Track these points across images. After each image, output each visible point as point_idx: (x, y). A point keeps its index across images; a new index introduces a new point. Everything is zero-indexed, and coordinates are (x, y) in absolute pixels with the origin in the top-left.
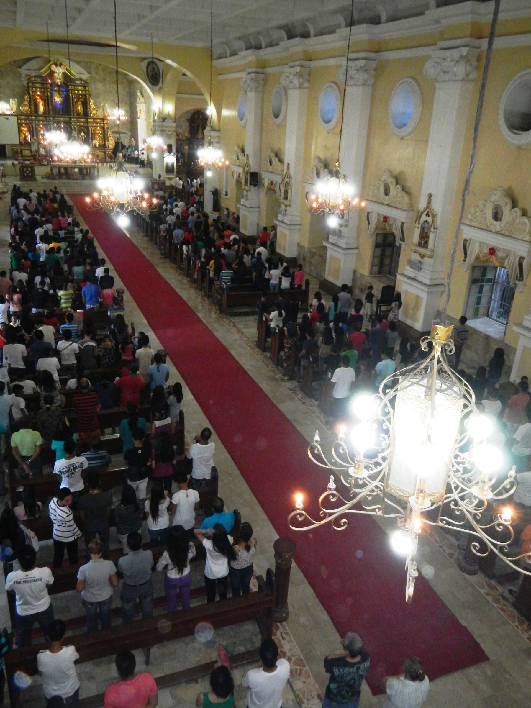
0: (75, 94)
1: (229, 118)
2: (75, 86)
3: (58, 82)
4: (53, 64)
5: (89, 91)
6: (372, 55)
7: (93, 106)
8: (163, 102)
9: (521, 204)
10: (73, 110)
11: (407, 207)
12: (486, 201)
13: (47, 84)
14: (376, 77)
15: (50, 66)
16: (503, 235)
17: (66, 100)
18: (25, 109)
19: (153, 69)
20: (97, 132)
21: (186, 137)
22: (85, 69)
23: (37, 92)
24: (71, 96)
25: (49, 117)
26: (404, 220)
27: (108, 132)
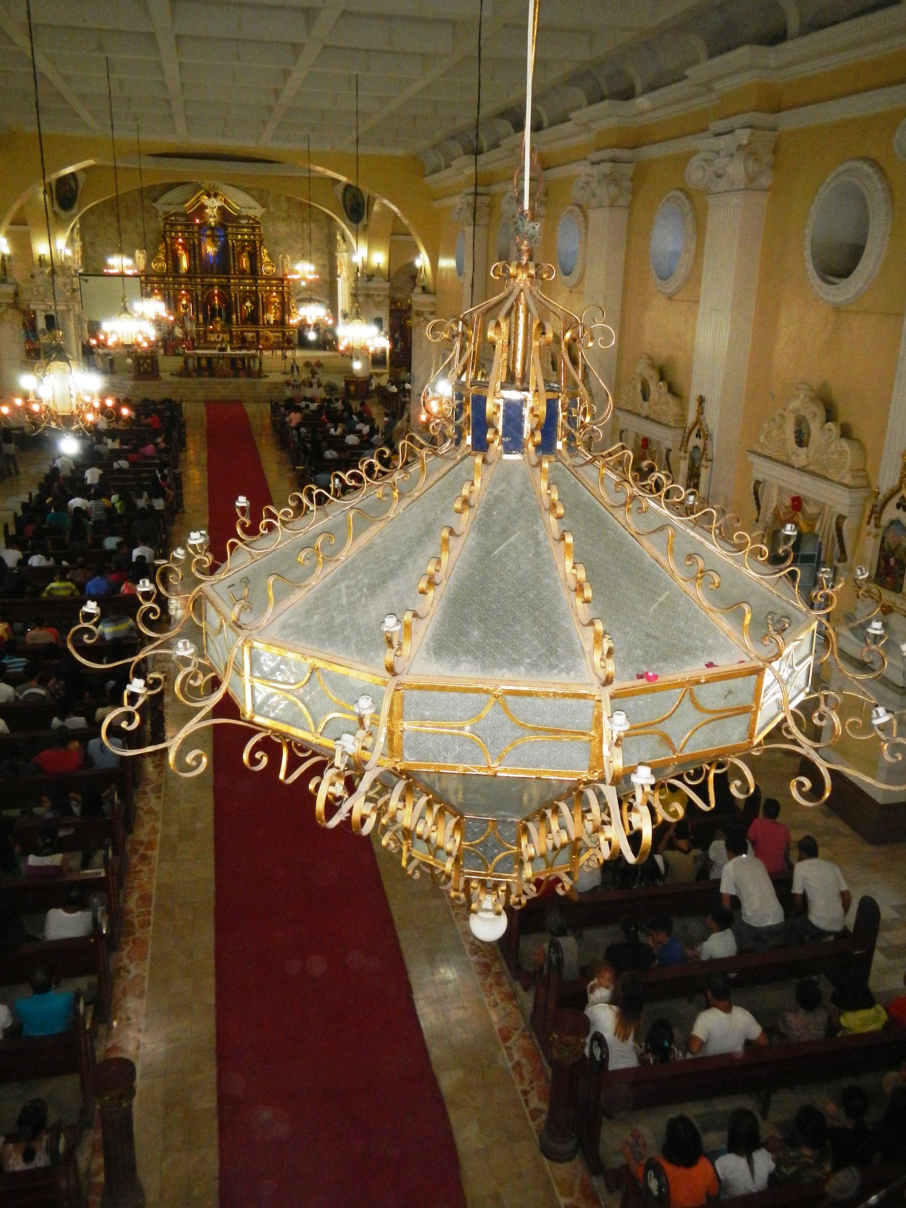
0: (237, 241)
1: (447, 270)
4: (203, 194)
6: (625, 154)
7: (266, 259)
8: (370, 249)
9: (842, 417)
10: (234, 266)
11: (675, 420)
12: (785, 409)
13: (192, 225)
14: (634, 192)
16: (813, 473)
17: (224, 252)
18: (159, 266)
22: (257, 201)
23: (177, 239)
25: (196, 278)
26: (668, 444)
27: (289, 300)
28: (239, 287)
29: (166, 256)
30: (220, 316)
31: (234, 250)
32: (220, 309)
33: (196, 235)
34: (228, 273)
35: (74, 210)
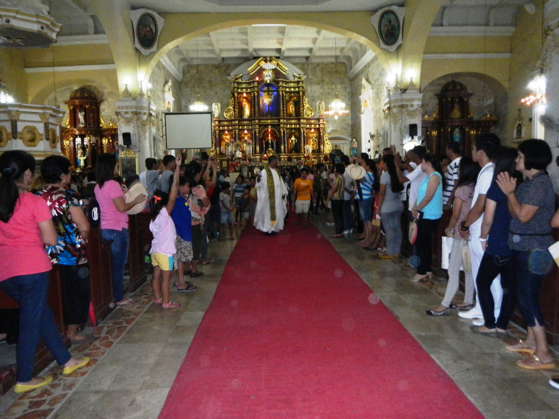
0: (286, 92)
3: (268, 79)
4: (262, 60)
5: (303, 87)
7: (307, 106)
8: (404, 65)
13: (253, 82)
15: (260, 61)
17: (276, 104)
19: (390, 21)
20: (311, 135)
21: (435, 118)
23: (242, 93)
24: (281, 94)
25: (255, 120)
27: (324, 134)
28: (286, 125)
29: (234, 108)
30: (272, 147)
31: (283, 99)
32: (272, 143)
33: (256, 88)
34: (280, 116)
35: (154, 49)
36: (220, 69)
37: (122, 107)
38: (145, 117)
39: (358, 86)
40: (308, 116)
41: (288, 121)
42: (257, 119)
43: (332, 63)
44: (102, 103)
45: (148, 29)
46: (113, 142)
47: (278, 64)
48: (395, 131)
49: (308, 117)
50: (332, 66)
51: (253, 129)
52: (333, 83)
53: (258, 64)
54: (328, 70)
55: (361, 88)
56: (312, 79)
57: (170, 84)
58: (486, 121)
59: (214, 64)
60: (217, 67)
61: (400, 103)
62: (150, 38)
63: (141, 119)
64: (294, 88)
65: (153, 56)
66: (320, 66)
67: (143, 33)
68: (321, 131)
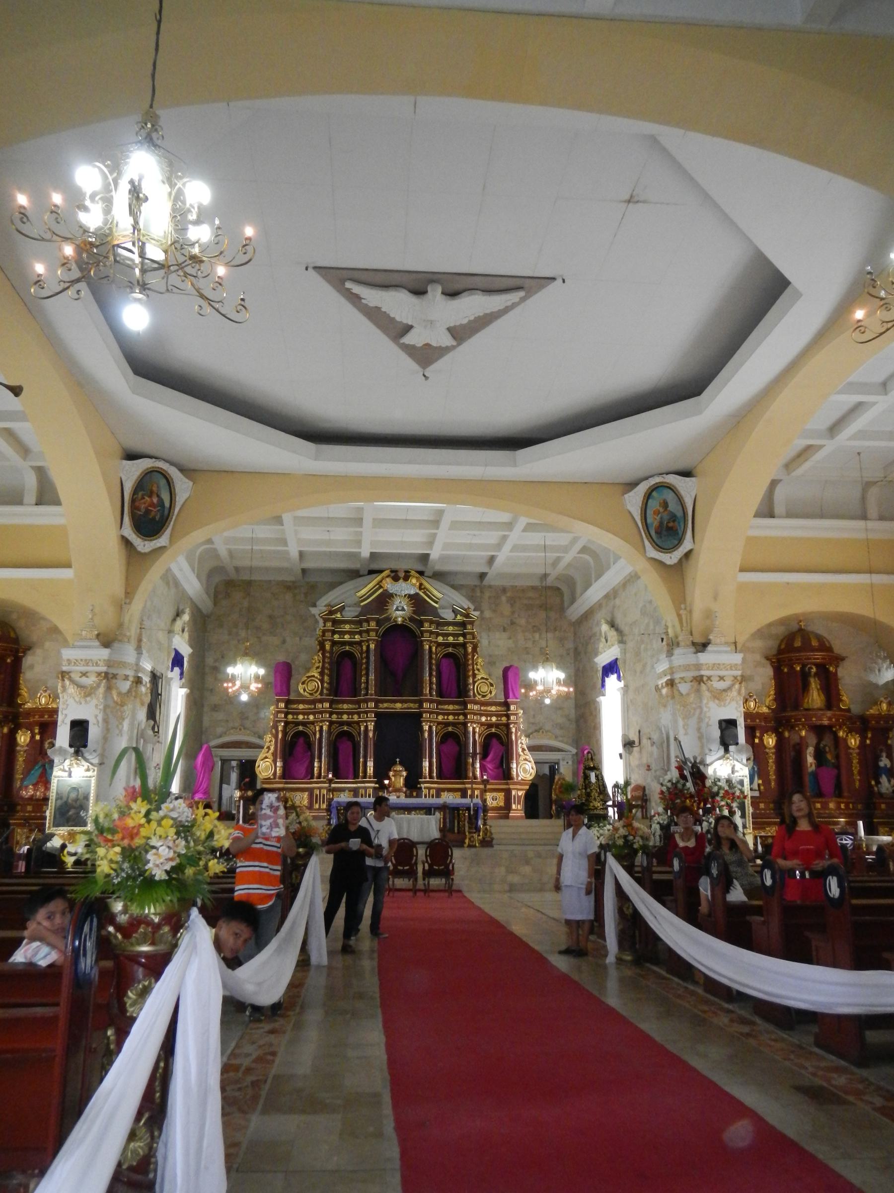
0: (439, 645)
2: (439, 624)
4: (388, 576)
5: (472, 634)
19: (665, 505)
25: (366, 701)
29: (322, 674)
31: (431, 658)
33: (373, 634)
35: (162, 540)
36: (296, 591)
37: (76, 662)
38: (125, 686)
39: (590, 638)
40: (484, 696)
41: (439, 707)
42: (371, 700)
43: (534, 588)
44: (29, 652)
45: (155, 500)
46: (42, 741)
47: (421, 584)
48: (686, 734)
49: (483, 699)
50: (531, 594)
51: (362, 721)
52: (536, 629)
53: (378, 584)
54: (526, 602)
55: (599, 640)
56: (491, 619)
57: (186, 617)
58: (879, 717)
59: (283, 582)
60: (289, 587)
61: (696, 674)
62: (157, 518)
63: (117, 689)
64: (455, 635)
65: (163, 554)
66: (509, 594)
67: (143, 506)
68: (514, 730)
